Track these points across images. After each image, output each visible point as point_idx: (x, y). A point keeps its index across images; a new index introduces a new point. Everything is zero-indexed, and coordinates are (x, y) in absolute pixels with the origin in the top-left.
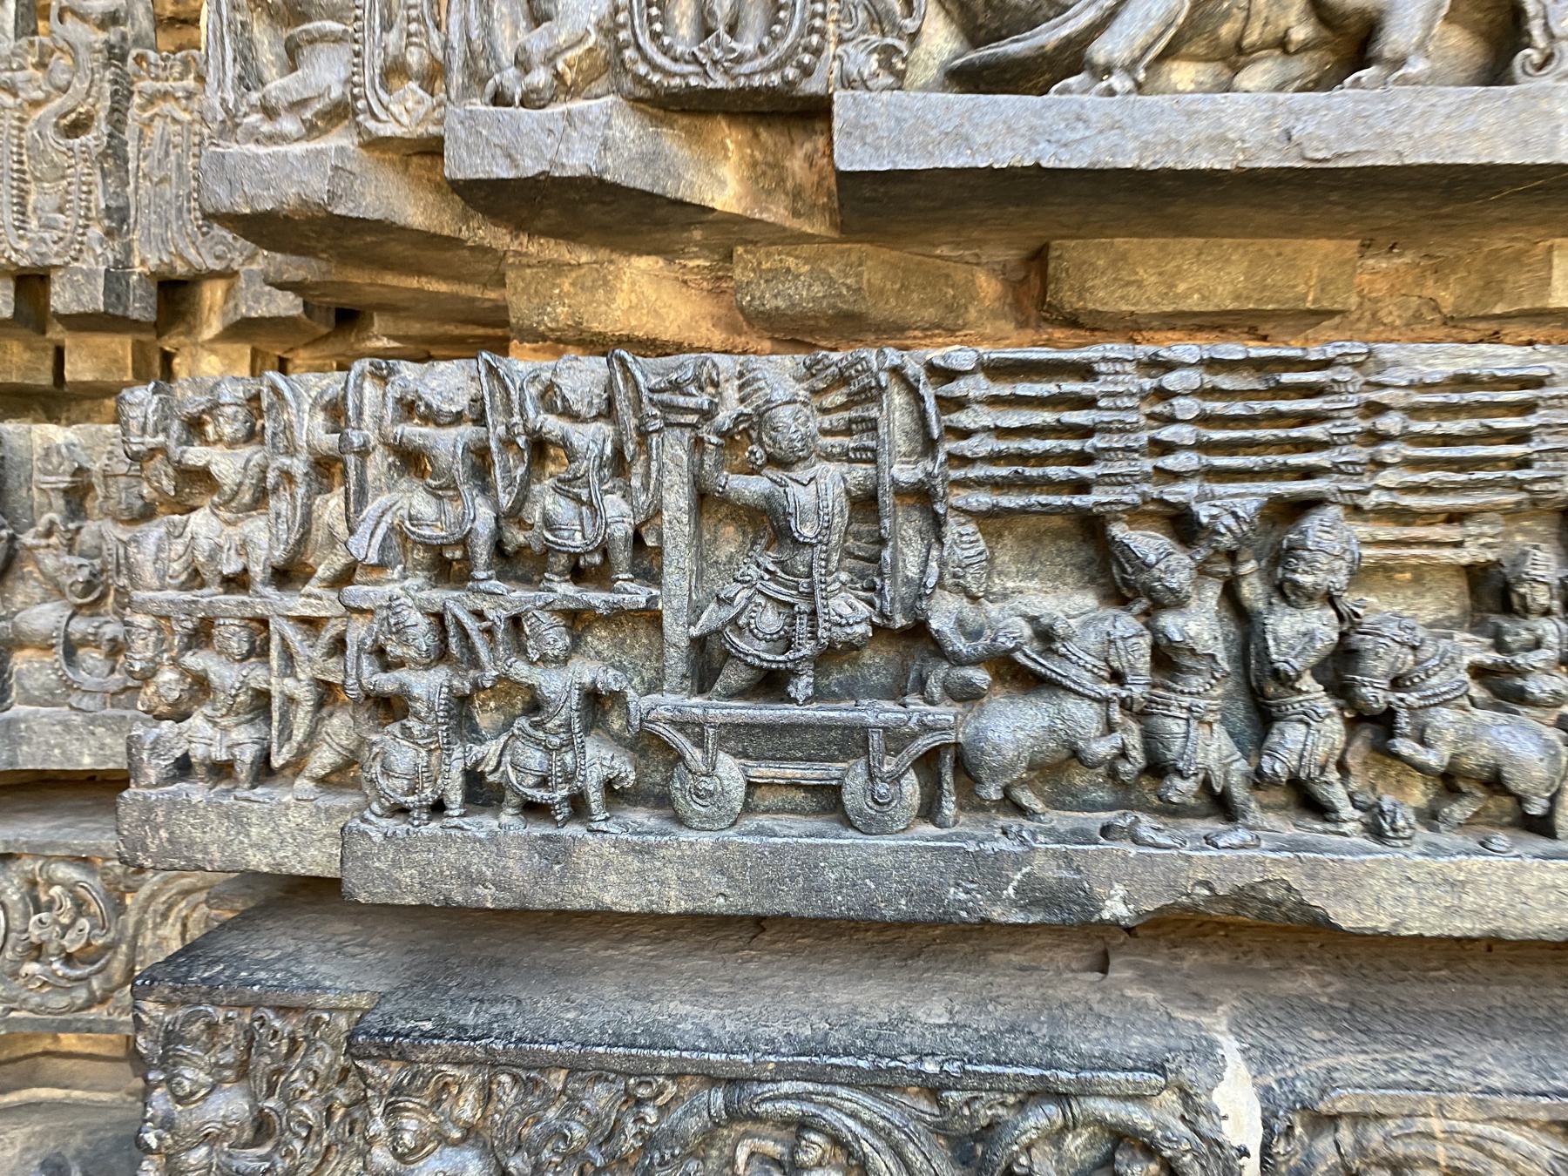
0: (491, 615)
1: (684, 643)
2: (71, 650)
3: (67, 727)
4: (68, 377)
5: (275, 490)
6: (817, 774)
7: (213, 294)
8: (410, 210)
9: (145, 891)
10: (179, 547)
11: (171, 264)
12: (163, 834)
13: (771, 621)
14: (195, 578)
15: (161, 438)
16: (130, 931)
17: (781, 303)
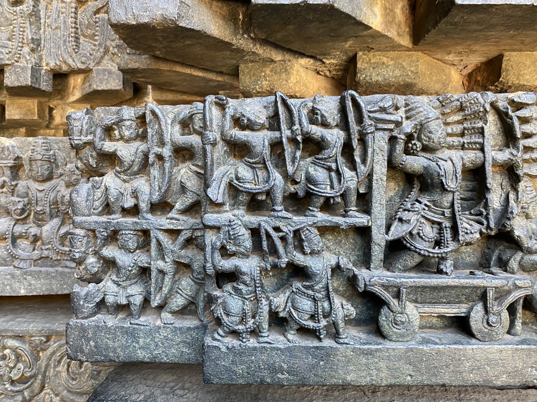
0: (285, 229)
1: (383, 244)
2: (14, 239)
3: (13, 276)
4: (7, 117)
5: (153, 165)
6: (455, 311)
7: (76, 81)
8: (213, 27)
9: (50, 350)
10: (99, 193)
11: (60, 66)
12: (92, 343)
13: (430, 232)
14: (107, 208)
15: (90, 137)
16: (43, 369)
17: (380, 79)
